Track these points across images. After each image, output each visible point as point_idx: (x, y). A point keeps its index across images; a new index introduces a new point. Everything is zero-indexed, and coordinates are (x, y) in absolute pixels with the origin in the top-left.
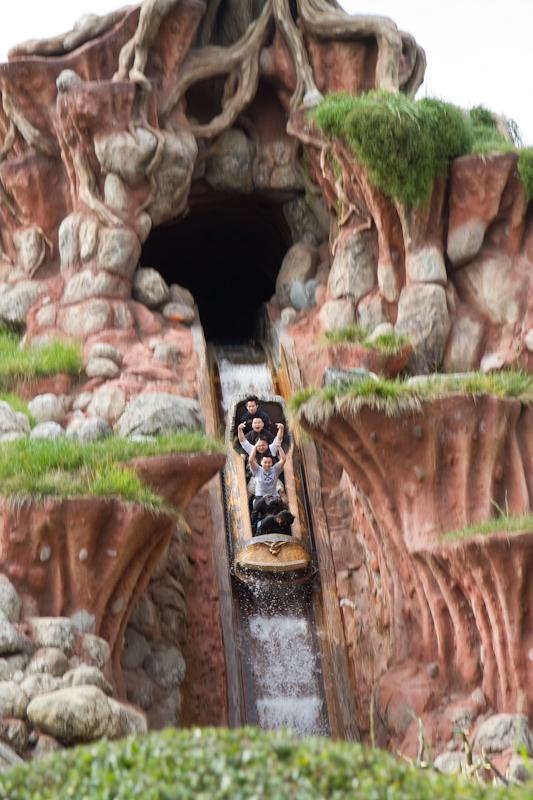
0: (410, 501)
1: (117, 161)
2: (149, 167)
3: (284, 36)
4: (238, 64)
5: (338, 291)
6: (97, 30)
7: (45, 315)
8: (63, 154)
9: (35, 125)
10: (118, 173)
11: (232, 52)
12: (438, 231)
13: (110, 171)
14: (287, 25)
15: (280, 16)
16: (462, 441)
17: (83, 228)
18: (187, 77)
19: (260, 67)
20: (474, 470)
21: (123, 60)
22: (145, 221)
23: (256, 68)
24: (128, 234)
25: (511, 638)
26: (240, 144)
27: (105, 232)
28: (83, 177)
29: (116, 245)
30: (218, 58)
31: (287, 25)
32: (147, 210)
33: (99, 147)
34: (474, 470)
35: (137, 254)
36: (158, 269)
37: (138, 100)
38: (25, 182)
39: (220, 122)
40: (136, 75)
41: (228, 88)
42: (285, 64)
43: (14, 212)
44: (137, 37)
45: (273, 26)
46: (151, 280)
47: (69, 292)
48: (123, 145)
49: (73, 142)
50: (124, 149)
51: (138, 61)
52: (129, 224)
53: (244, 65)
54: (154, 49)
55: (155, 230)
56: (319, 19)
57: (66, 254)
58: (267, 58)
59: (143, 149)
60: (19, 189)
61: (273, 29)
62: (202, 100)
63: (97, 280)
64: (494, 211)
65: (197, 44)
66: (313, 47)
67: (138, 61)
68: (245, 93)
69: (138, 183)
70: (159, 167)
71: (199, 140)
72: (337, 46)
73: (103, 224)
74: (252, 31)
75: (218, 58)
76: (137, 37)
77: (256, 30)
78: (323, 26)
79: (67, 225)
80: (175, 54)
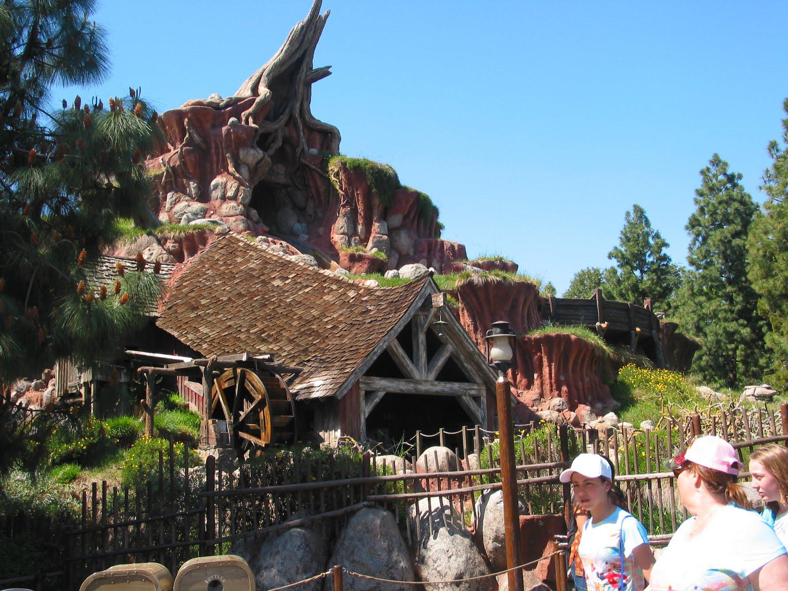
3: (296, 126)
4: (276, 130)
8: (213, 150)
10: (248, 165)
11: (275, 125)
12: (384, 217)
15: (297, 116)
16: (522, 300)
36: (254, 208)
41: (271, 138)
42: (295, 135)
43: (184, 171)
44: (251, 110)
45: (291, 117)
46: (254, 212)
50: (254, 154)
53: (280, 131)
64: (406, 212)
68: (279, 143)
72: (316, 133)
76: (251, 110)
77: (284, 118)
78: (313, 124)
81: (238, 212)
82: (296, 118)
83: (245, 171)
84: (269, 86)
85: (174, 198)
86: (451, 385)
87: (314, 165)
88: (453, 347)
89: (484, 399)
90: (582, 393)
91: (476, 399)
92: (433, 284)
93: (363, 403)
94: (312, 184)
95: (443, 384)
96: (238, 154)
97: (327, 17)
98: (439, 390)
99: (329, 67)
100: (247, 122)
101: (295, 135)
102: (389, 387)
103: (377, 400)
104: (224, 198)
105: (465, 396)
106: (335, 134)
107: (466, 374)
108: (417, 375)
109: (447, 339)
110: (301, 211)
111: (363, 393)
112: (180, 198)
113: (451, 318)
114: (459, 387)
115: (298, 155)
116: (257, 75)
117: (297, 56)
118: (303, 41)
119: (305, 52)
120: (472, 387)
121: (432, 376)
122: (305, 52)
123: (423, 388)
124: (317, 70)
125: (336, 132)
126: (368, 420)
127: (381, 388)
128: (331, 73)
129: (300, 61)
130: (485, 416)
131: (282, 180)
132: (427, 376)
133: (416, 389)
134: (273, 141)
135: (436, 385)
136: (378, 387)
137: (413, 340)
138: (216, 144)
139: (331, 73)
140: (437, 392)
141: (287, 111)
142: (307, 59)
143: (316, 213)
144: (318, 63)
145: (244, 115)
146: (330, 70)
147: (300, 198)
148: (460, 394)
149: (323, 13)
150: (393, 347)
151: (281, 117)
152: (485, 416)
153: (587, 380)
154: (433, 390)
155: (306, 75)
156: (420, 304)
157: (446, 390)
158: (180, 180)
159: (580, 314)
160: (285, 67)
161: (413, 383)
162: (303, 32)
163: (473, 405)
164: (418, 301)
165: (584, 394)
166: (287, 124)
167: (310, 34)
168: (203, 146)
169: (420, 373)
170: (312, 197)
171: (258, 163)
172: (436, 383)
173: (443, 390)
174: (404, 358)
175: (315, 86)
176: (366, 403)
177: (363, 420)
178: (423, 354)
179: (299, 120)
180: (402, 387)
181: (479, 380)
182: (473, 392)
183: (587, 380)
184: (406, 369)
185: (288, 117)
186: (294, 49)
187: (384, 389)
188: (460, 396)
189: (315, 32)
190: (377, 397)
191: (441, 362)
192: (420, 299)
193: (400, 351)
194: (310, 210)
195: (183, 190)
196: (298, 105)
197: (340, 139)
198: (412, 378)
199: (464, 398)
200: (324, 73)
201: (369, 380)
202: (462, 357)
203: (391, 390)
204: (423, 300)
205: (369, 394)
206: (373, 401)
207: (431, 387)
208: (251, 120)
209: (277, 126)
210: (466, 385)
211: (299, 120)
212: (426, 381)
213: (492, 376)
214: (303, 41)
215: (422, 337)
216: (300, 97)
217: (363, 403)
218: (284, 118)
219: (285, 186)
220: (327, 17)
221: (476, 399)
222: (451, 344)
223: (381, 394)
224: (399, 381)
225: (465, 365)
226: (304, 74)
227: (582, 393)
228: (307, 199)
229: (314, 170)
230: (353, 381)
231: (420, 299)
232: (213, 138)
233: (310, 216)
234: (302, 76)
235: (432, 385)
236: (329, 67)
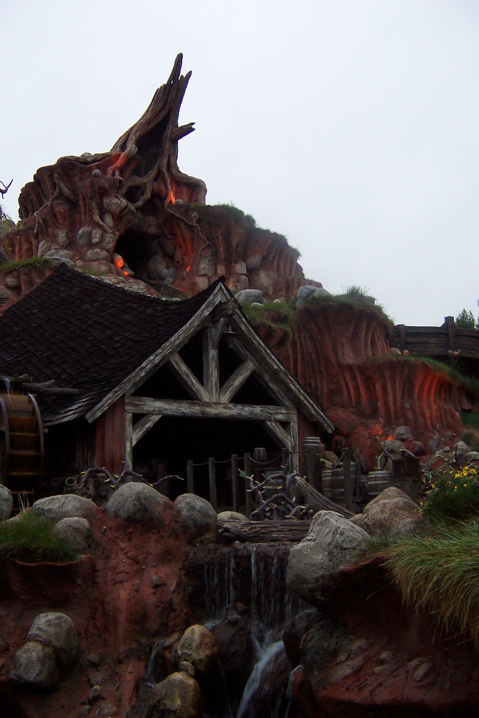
0: (343, 345)
2: (124, 213)
4: (145, 184)
5: (202, 273)
6: (99, 159)
9: (69, 190)
10: (111, 213)
13: (108, 212)
17: (94, 232)
19: (153, 188)
20: (366, 337)
23: (152, 187)
25: (399, 397)
27: (107, 234)
29: (110, 241)
32: (118, 230)
34: (366, 337)
38: (62, 210)
42: (163, 188)
45: (160, 174)
49: (92, 198)
53: (148, 185)
59: (123, 205)
60: (60, 212)
61: (160, 174)
63: (102, 253)
68: (148, 195)
74: (151, 174)
77: (153, 173)
82: (164, 173)
83: (109, 220)
84: (137, 144)
85: (44, 247)
86: (251, 408)
87: (179, 214)
88: (255, 365)
89: (294, 425)
90: (429, 421)
91: (285, 424)
92: (225, 291)
93: (129, 428)
94: (178, 232)
95: (239, 407)
96: (102, 204)
98: (235, 414)
99: (193, 124)
100: (113, 174)
101: (163, 188)
102: (165, 409)
103: (149, 425)
104: (91, 245)
105: (270, 421)
106: (201, 186)
107: (273, 396)
108: (205, 396)
109: (247, 355)
110: (170, 257)
111: (129, 416)
112: (50, 247)
113: (249, 330)
114: (262, 411)
115: (166, 206)
117: (162, 115)
118: (166, 101)
119: (170, 111)
120: (279, 411)
121: (225, 398)
122: (170, 111)
123: (213, 411)
124: (181, 127)
125: (202, 184)
126: (135, 449)
127: (154, 410)
128: (194, 130)
130: (295, 444)
131: (152, 230)
132: (219, 398)
133: (203, 412)
134: (143, 194)
135: (231, 408)
136: (151, 410)
137: (204, 356)
138: (83, 195)
139: (194, 130)
140: (232, 415)
141: (156, 167)
142: (172, 118)
143: (183, 259)
144: (182, 121)
145: (110, 170)
146: (193, 126)
147: (169, 246)
148: (262, 418)
149: (184, 72)
150: (174, 364)
151: (150, 172)
152: (295, 444)
153: (434, 407)
154: (226, 414)
155: (172, 133)
156: (207, 313)
157: (244, 413)
158: (50, 230)
159: (431, 342)
160: (151, 126)
161: (199, 405)
162: (166, 92)
163: (279, 432)
164: (204, 309)
165: (432, 422)
166: (156, 179)
167: (173, 94)
168: (72, 197)
169: (211, 394)
170: (180, 245)
172: (231, 406)
173: (239, 414)
174: (188, 376)
175: (181, 142)
176: (134, 430)
177: (128, 449)
178: (213, 373)
179: (166, 174)
180: (184, 410)
181: (287, 403)
182: (280, 417)
183: (434, 407)
184: (190, 388)
185: (156, 172)
186: (159, 108)
187: (159, 412)
188: (263, 421)
190: (149, 421)
191: (238, 381)
192: (207, 307)
193: (183, 368)
194: (178, 257)
195: (53, 238)
196: (165, 160)
197: (206, 191)
198: (198, 399)
199: (268, 423)
200: (189, 129)
201: (141, 401)
202: (267, 377)
203: (169, 413)
204: (211, 309)
205: (138, 418)
206: (143, 426)
207: (224, 410)
208: (117, 173)
209: (145, 181)
210: (271, 409)
211: (166, 174)
212: (216, 404)
213: (302, 398)
214: (166, 101)
215: (213, 353)
216: (166, 153)
217: (129, 428)
218: (153, 173)
219: (156, 237)
221: (285, 424)
222: (252, 362)
223: (156, 418)
224: (180, 403)
225: (271, 385)
226: (170, 130)
227: (429, 421)
228: (175, 248)
229: (179, 218)
230: (110, 401)
231: (207, 307)
232: (80, 190)
233: (178, 262)
234: (168, 133)
235: (225, 408)
236: (193, 124)
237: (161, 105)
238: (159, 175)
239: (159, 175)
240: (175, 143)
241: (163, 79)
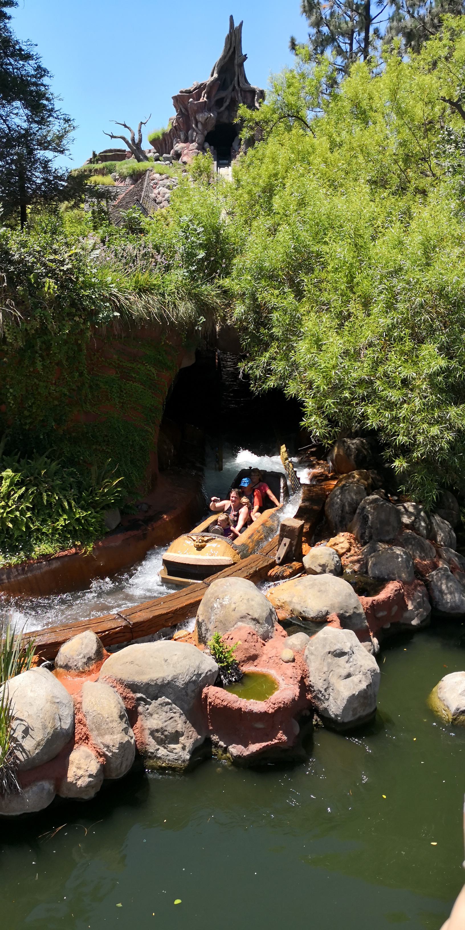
1: (200, 119)
7: (185, 152)
14: (237, 87)
18: (216, 99)
21: (203, 95)
22: (206, 133)
24: (202, 136)
26: (226, 113)
28: (194, 122)
30: (223, 94)
31: (237, 87)
33: (197, 116)
35: (204, 139)
37: (205, 105)
39: (222, 109)
40: (205, 99)
41: (225, 100)
45: (234, 87)
47: (190, 147)
48: (201, 117)
51: (206, 95)
52: (202, 134)
54: (209, 93)
55: (208, 133)
56: (244, 87)
57: (190, 138)
58: (233, 93)
59: (206, 117)
62: (220, 102)
65: (219, 90)
66: (242, 93)
67: (206, 95)
68: (227, 103)
69: (204, 125)
70: (209, 121)
71: (218, 113)
73: (197, 133)
75: (223, 94)
77: (231, 88)
79: (190, 132)
80: (214, 93)
81: (194, 148)
83: (200, 126)
97: (241, 25)
116: (213, 66)
122: (234, 48)
129: (234, 52)
149: (236, 24)
167: (233, 38)
168: (186, 113)
171: (206, 120)
186: (228, 48)
189: (235, 36)
196: (236, 78)
200: (245, 58)
216: (237, 74)
220: (241, 25)
236: (246, 55)
237: (229, 46)
238: (234, 89)
239: (234, 89)
240: (241, 65)
241: (227, 32)
